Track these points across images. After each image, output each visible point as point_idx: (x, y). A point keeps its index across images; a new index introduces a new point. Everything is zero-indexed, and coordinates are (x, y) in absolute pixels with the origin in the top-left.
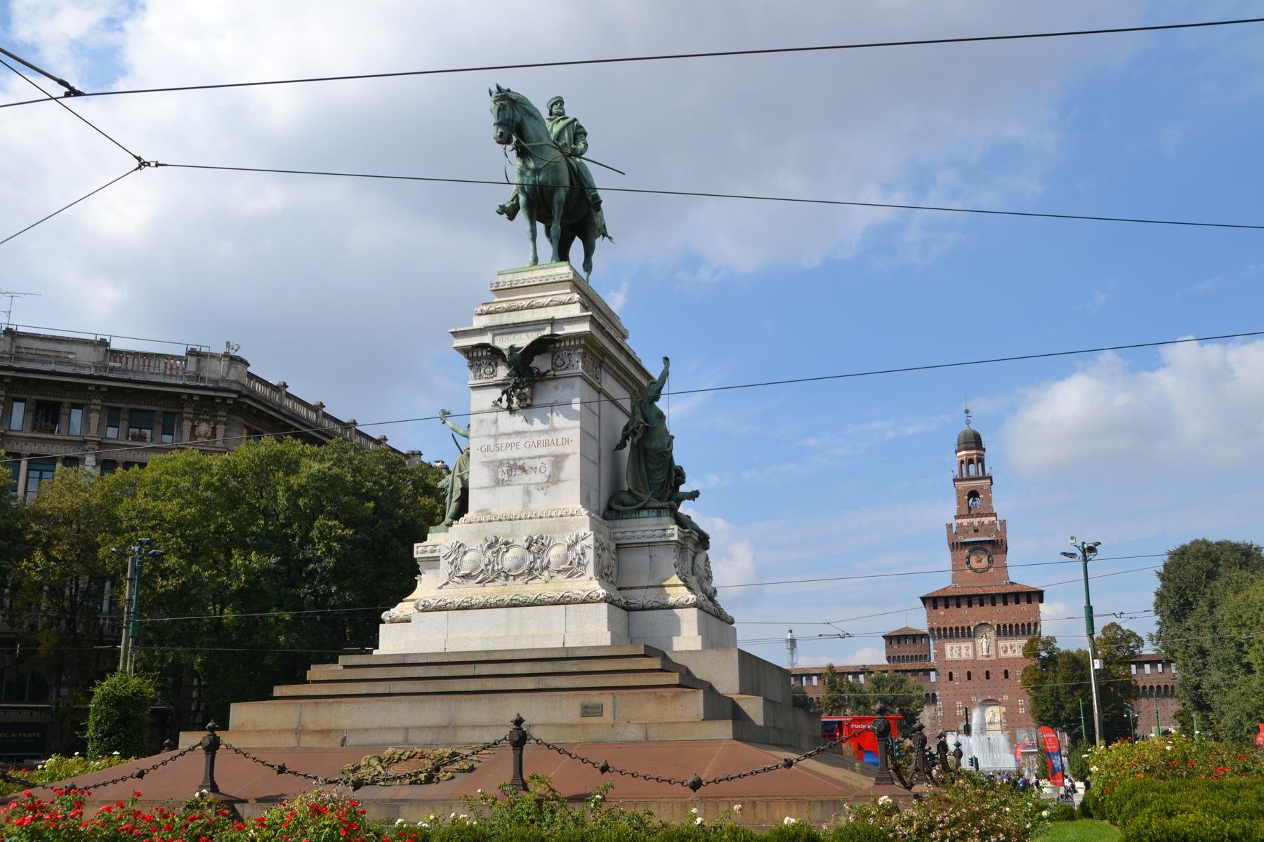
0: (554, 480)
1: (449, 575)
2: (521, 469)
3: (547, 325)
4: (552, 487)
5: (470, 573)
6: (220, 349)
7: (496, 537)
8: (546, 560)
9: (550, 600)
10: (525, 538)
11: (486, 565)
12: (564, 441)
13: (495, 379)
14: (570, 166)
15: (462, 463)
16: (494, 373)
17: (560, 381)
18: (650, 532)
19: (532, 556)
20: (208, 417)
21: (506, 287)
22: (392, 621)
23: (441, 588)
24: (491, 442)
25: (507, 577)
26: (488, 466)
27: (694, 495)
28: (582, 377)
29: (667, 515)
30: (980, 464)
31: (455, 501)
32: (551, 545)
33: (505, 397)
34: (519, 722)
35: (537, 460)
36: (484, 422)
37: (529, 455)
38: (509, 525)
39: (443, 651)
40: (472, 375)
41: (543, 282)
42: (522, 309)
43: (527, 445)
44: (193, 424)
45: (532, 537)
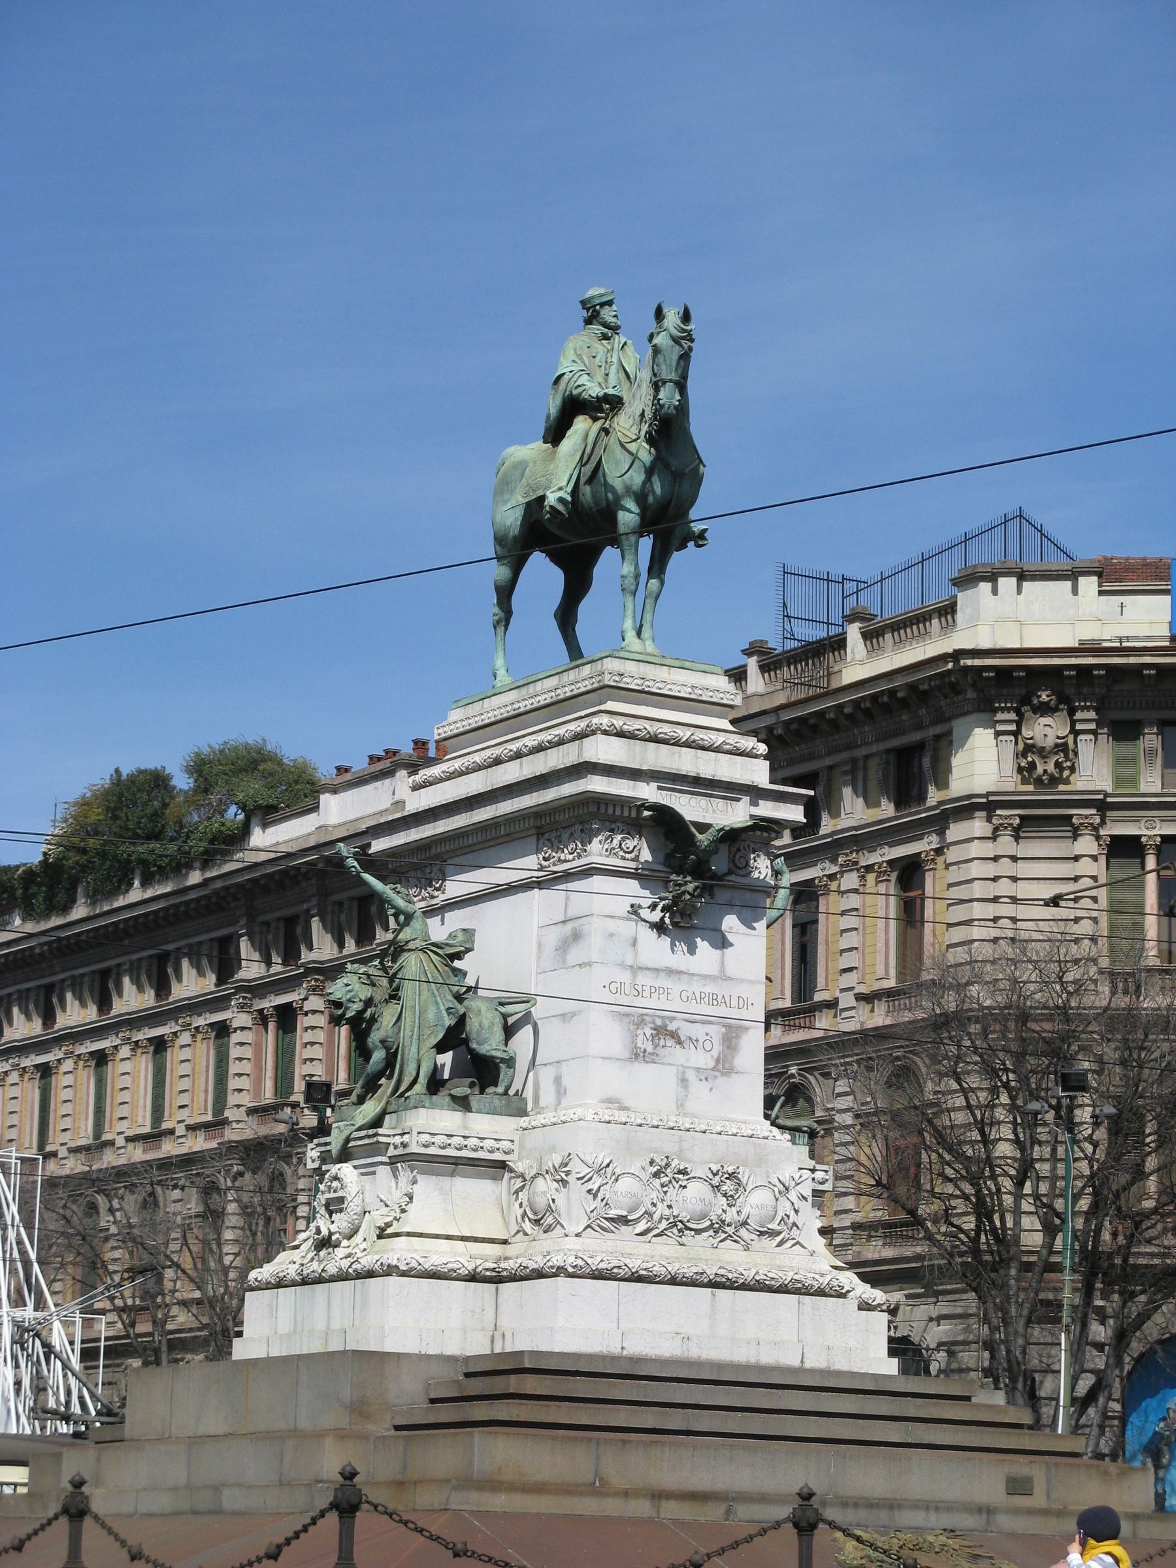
2: (673, 1037)
4: (722, 1081)
9: (773, 1283)
24: (626, 977)
41: (693, 696)
42: (677, 743)
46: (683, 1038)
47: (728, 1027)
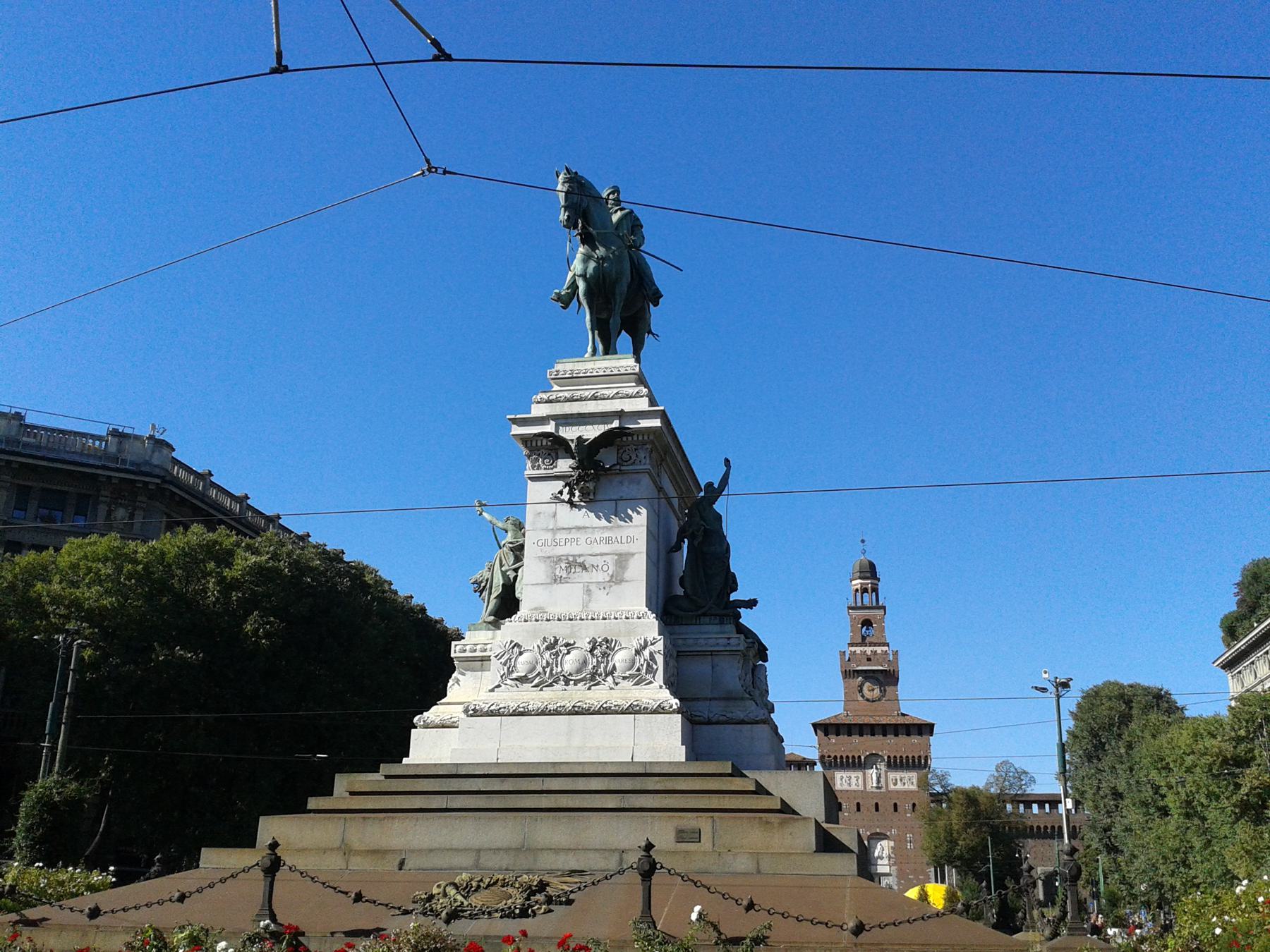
0: (617, 579)
1: (502, 677)
3: (615, 417)
4: (615, 588)
5: (526, 676)
6: (145, 432)
7: (555, 637)
8: (611, 665)
10: (588, 640)
11: (544, 668)
12: (629, 540)
13: (555, 470)
14: (631, 258)
15: (503, 557)
16: (554, 464)
17: (625, 476)
18: (714, 640)
19: (595, 660)
20: (126, 502)
21: (567, 376)
22: (426, 726)
23: (492, 690)
24: (549, 536)
25: (567, 683)
26: (545, 561)
27: (751, 604)
28: (649, 473)
29: (730, 623)
30: (874, 593)
31: (495, 598)
32: (616, 648)
33: (566, 490)
34: (649, 847)
35: (599, 557)
36: (542, 515)
37: (590, 553)
38: (569, 626)
39: (495, 761)
40: (529, 464)
42: (586, 399)
43: (589, 542)
44: (110, 507)
45: (595, 639)
46: (587, 566)
47: (620, 555)
